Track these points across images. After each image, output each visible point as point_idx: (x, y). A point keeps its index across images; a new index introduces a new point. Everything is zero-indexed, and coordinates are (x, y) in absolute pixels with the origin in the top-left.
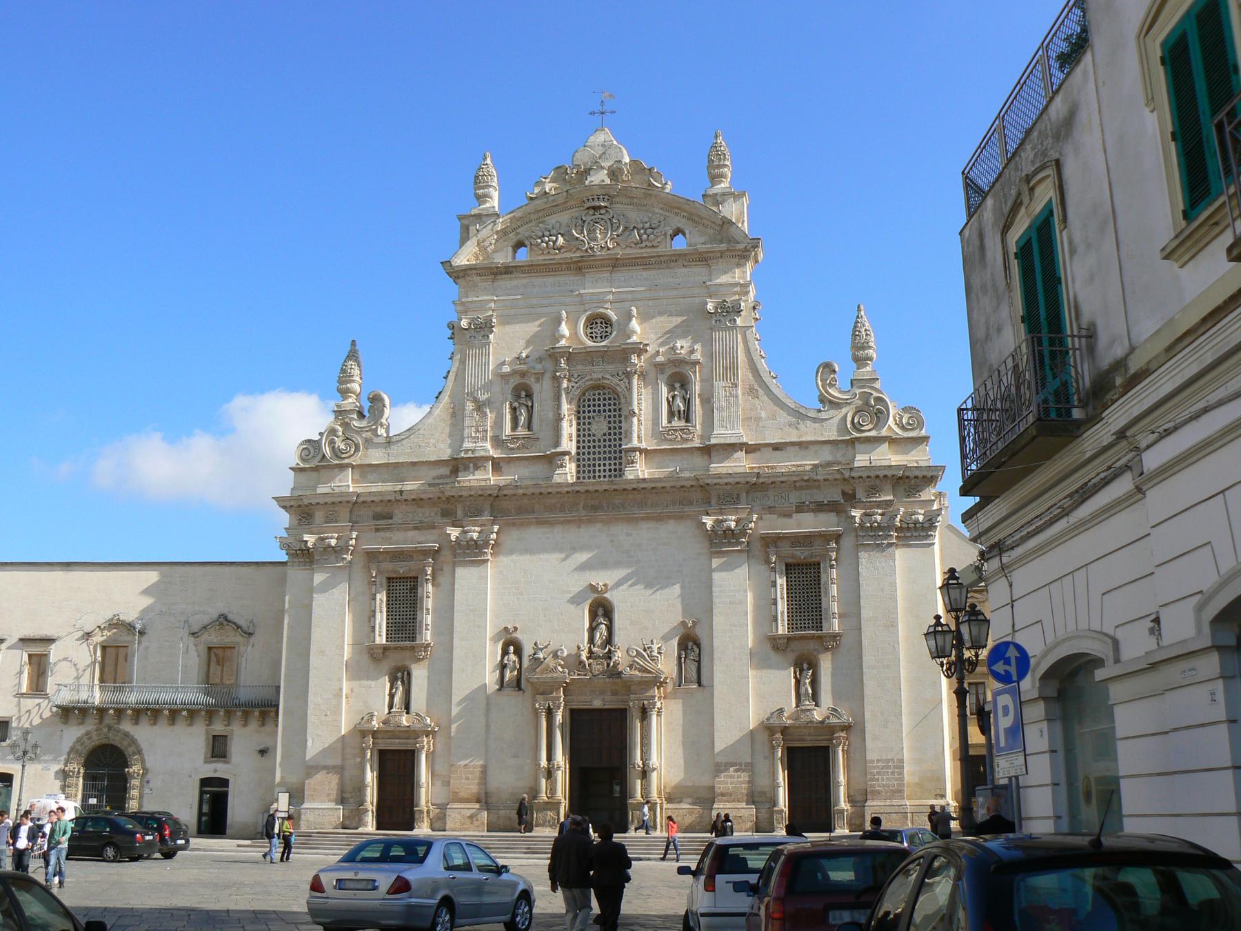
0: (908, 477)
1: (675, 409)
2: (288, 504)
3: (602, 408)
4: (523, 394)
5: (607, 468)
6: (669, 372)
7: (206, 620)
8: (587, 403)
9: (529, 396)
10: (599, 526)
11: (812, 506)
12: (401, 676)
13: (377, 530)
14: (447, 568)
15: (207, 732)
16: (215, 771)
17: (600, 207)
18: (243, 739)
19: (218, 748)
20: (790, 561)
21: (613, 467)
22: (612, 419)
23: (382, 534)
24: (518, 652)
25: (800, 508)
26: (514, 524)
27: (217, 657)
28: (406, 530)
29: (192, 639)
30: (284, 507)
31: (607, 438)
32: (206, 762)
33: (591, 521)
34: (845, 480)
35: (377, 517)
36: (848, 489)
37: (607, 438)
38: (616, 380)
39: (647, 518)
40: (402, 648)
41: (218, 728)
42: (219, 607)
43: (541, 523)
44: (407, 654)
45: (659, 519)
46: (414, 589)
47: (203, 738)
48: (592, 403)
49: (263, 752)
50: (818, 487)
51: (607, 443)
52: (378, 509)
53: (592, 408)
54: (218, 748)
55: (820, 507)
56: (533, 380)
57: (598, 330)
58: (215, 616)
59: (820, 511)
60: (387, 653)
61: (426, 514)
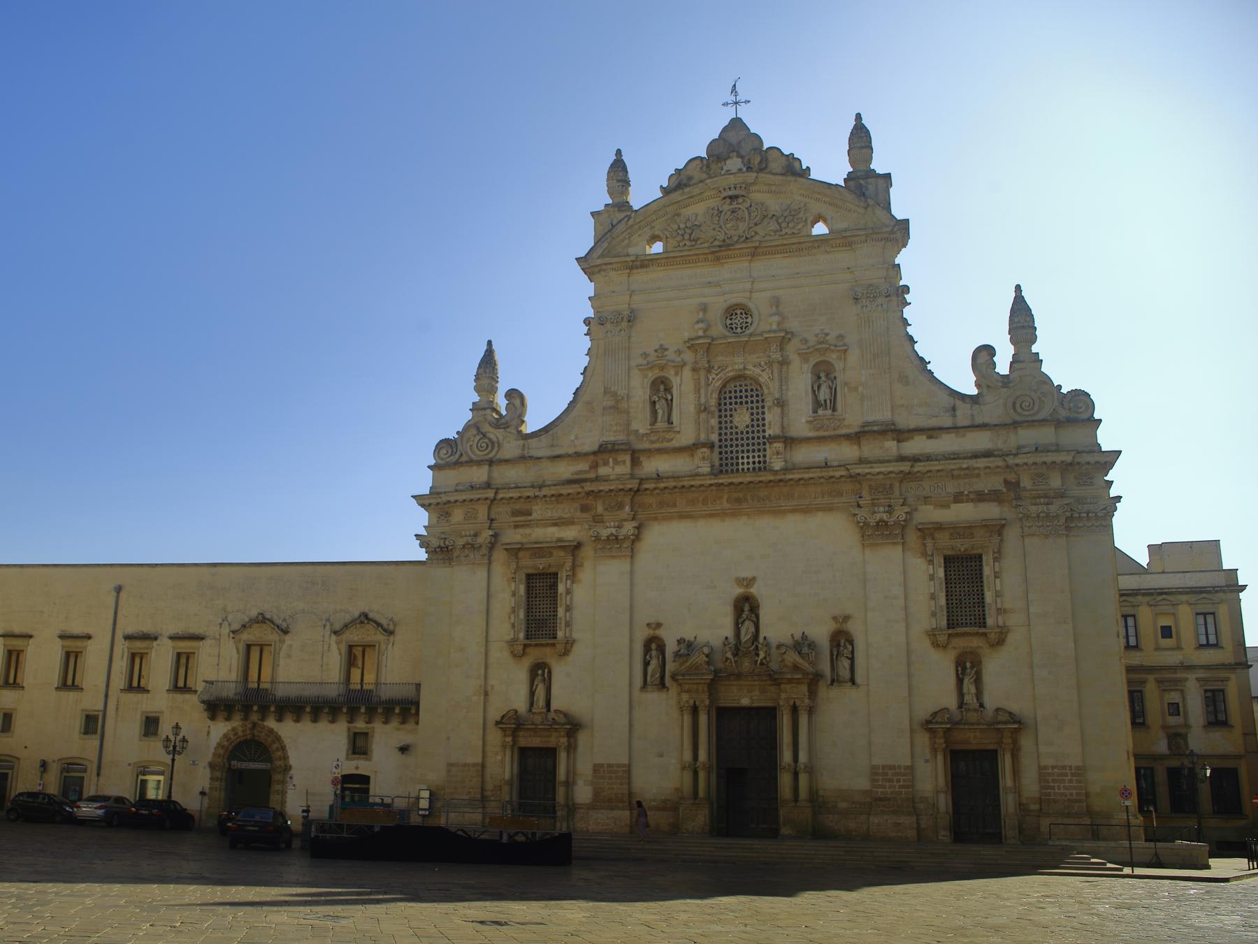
0: (1078, 463)
1: (822, 397)
2: (427, 502)
3: (744, 400)
4: (662, 387)
5: (751, 460)
6: (814, 360)
7: (348, 618)
8: (728, 395)
9: (668, 390)
10: (744, 519)
11: (972, 496)
12: (540, 673)
13: (516, 527)
14: (588, 565)
15: (349, 729)
16: (357, 768)
17: (737, 197)
18: (385, 737)
19: (359, 745)
20: (949, 553)
21: (757, 459)
22: (755, 411)
23: (520, 530)
24: (661, 649)
25: (958, 498)
26: (656, 519)
27: (353, 657)
28: (545, 526)
29: (334, 637)
30: (422, 506)
31: (750, 429)
32: (347, 758)
33: (735, 514)
34: (1007, 467)
35: (515, 513)
36: (1012, 477)
37: (750, 429)
38: (758, 371)
39: (794, 511)
40: (542, 645)
41: (360, 725)
42: (362, 606)
43: (682, 516)
44: (547, 650)
45: (807, 510)
46: (554, 586)
47: (345, 734)
48: (733, 395)
49: (404, 749)
50: (978, 476)
51: (750, 435)
52: (518, 506)
53: (733, 400)
54: (359, 745)
55: (980, 497)
56: (672, 372)
57: (738, 320)
58: (357, 614)
59: (980, 501)
60: (528, 650)
61: (565, 510)
